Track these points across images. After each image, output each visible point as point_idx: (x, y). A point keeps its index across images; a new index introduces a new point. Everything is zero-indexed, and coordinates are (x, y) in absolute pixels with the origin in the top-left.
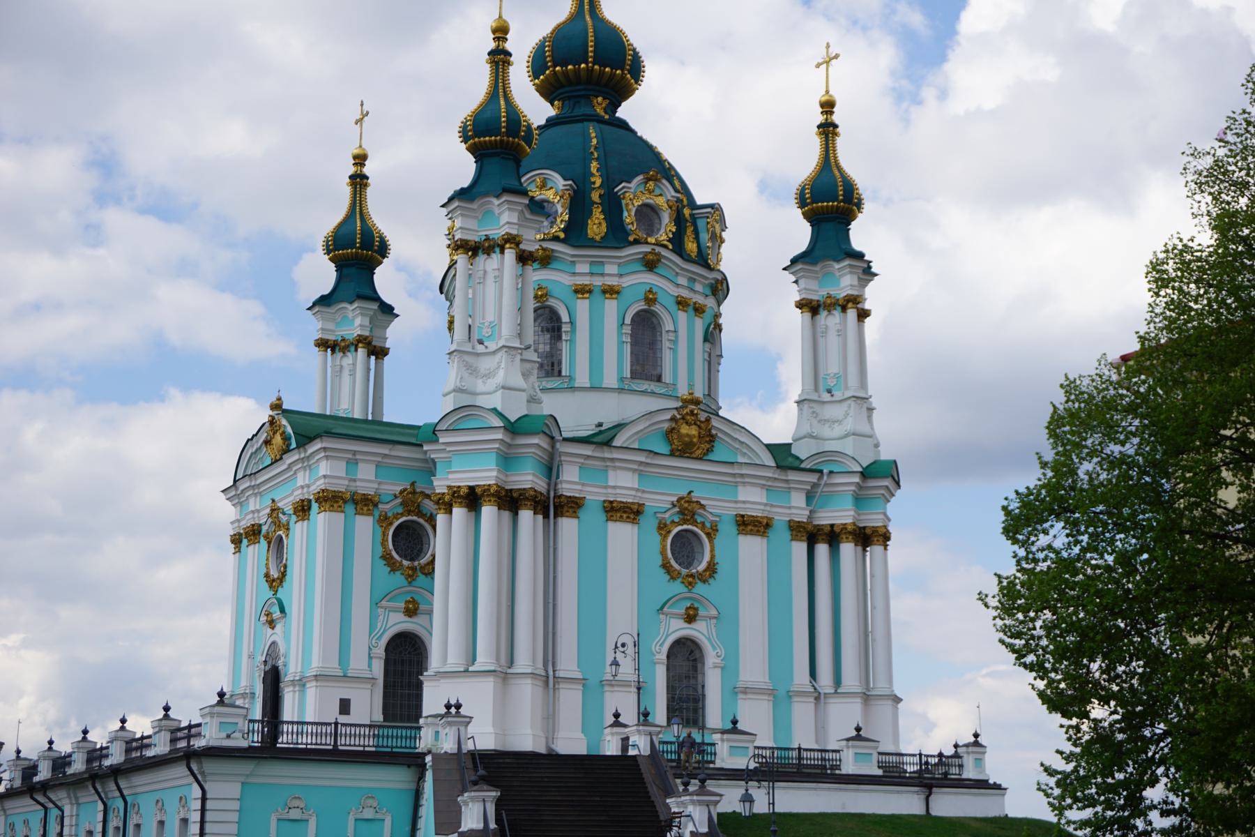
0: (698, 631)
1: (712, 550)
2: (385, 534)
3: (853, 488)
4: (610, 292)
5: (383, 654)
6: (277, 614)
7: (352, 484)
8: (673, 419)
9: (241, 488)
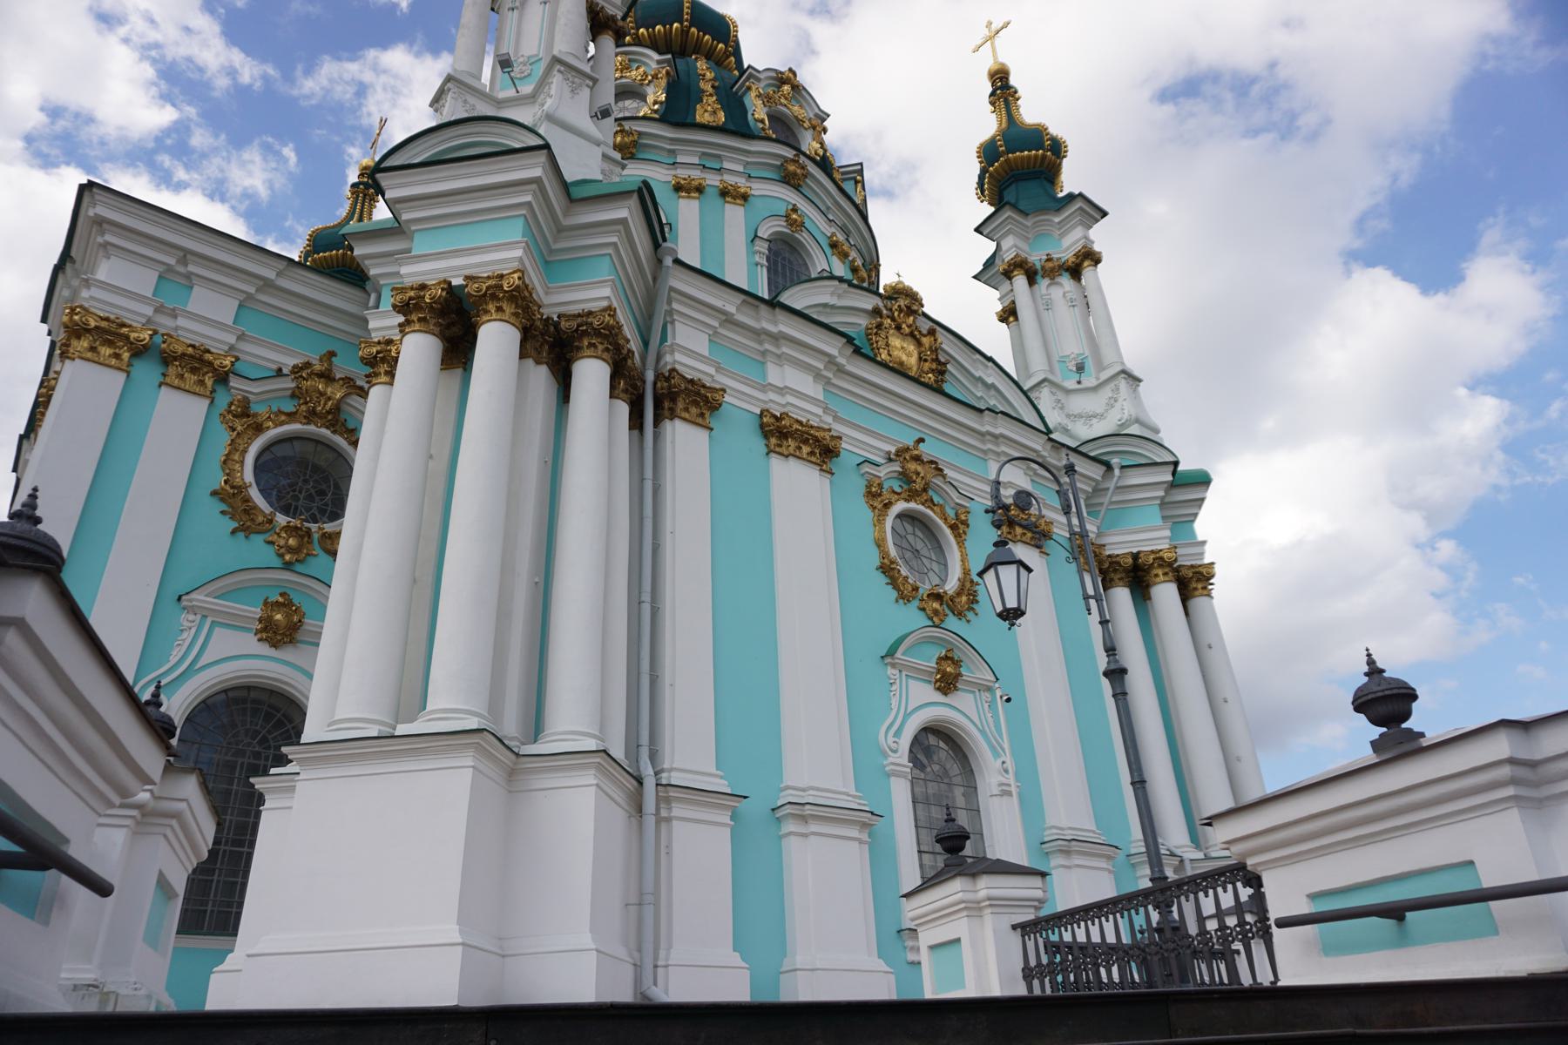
0: (962, 710)
3: (1162, 493)
8: (876, 312)
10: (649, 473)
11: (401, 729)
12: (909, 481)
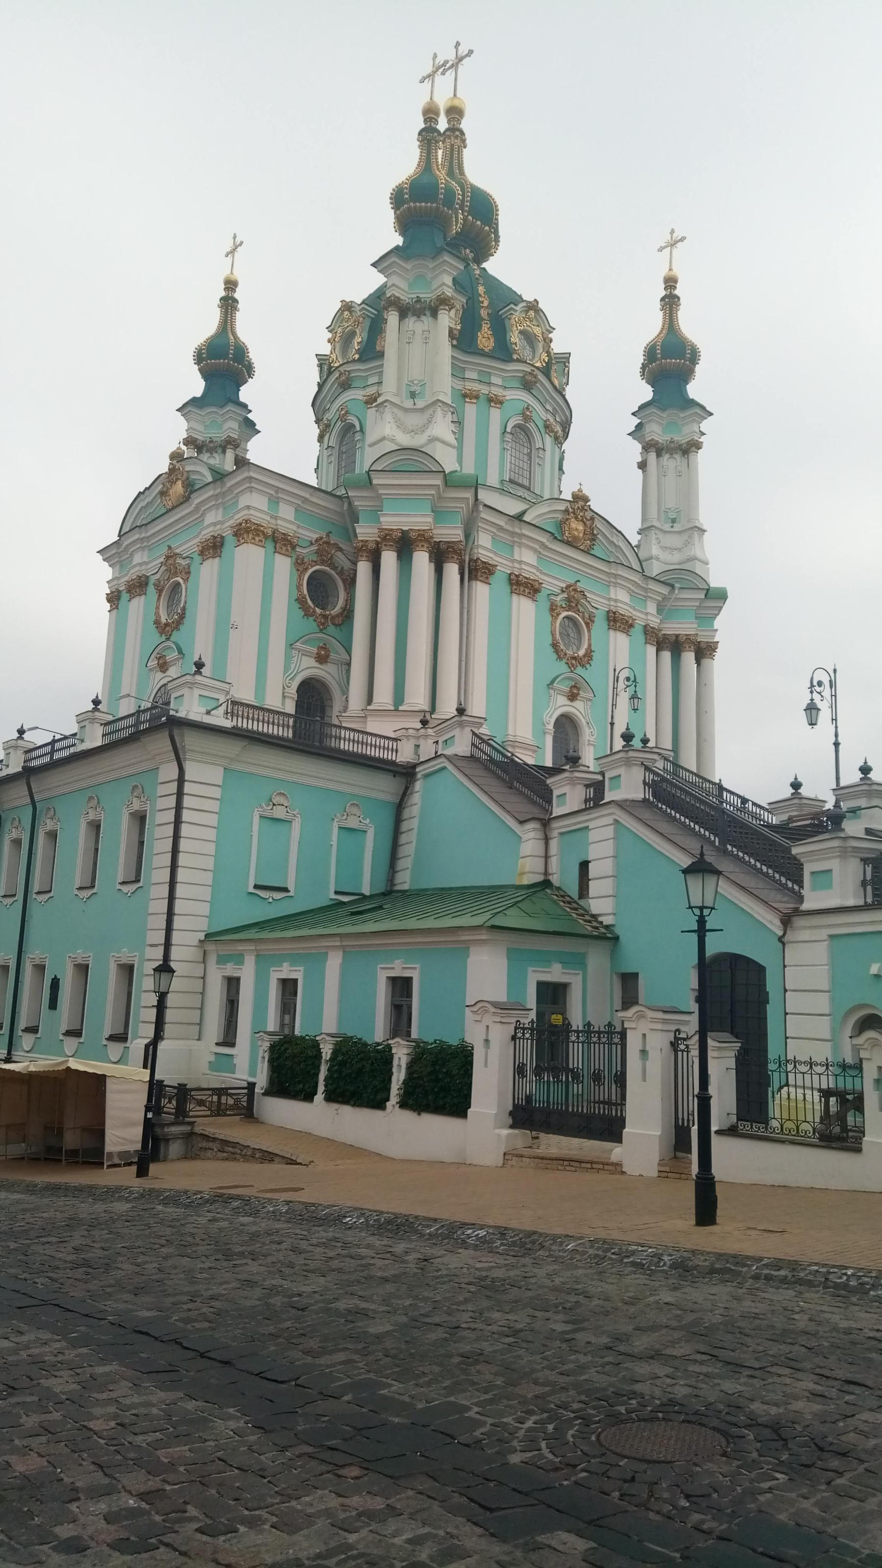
0: (578, 709)
1: (589, 639)
2: (300, 578)
5: (296, 696)
6: (172, 655)
7: (273, 521)
8: (566, 511)
9: (126, 543)
10: (466, 606)
11: (401, 708)
12: (570, 601)
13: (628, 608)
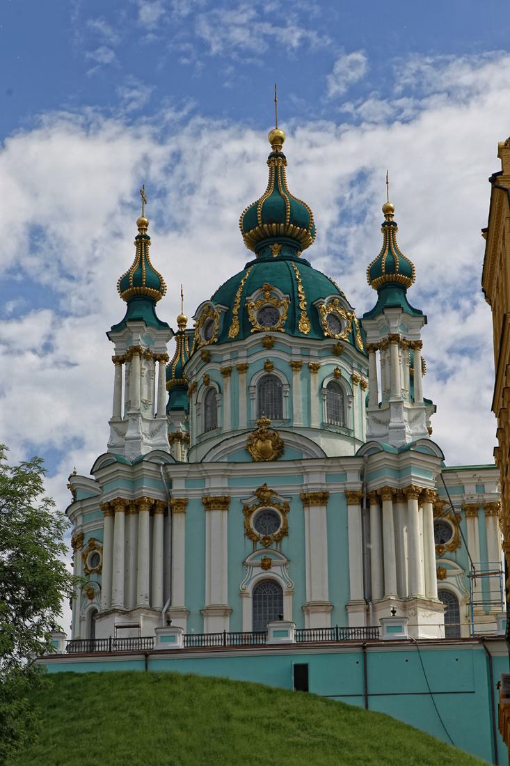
0: (276, 572)
4: (243, 368)
8: (250, 439)
13: (320, 487)
